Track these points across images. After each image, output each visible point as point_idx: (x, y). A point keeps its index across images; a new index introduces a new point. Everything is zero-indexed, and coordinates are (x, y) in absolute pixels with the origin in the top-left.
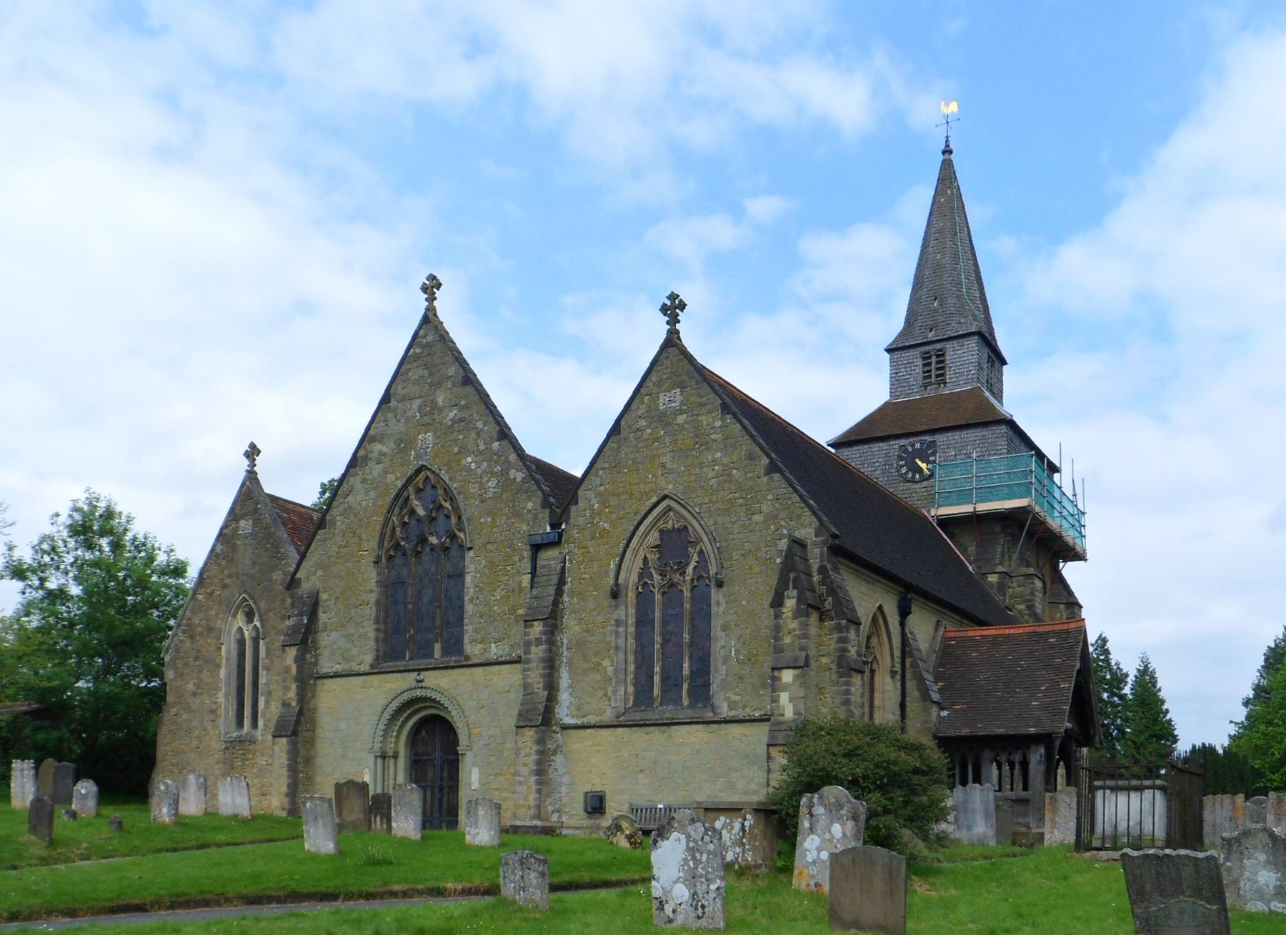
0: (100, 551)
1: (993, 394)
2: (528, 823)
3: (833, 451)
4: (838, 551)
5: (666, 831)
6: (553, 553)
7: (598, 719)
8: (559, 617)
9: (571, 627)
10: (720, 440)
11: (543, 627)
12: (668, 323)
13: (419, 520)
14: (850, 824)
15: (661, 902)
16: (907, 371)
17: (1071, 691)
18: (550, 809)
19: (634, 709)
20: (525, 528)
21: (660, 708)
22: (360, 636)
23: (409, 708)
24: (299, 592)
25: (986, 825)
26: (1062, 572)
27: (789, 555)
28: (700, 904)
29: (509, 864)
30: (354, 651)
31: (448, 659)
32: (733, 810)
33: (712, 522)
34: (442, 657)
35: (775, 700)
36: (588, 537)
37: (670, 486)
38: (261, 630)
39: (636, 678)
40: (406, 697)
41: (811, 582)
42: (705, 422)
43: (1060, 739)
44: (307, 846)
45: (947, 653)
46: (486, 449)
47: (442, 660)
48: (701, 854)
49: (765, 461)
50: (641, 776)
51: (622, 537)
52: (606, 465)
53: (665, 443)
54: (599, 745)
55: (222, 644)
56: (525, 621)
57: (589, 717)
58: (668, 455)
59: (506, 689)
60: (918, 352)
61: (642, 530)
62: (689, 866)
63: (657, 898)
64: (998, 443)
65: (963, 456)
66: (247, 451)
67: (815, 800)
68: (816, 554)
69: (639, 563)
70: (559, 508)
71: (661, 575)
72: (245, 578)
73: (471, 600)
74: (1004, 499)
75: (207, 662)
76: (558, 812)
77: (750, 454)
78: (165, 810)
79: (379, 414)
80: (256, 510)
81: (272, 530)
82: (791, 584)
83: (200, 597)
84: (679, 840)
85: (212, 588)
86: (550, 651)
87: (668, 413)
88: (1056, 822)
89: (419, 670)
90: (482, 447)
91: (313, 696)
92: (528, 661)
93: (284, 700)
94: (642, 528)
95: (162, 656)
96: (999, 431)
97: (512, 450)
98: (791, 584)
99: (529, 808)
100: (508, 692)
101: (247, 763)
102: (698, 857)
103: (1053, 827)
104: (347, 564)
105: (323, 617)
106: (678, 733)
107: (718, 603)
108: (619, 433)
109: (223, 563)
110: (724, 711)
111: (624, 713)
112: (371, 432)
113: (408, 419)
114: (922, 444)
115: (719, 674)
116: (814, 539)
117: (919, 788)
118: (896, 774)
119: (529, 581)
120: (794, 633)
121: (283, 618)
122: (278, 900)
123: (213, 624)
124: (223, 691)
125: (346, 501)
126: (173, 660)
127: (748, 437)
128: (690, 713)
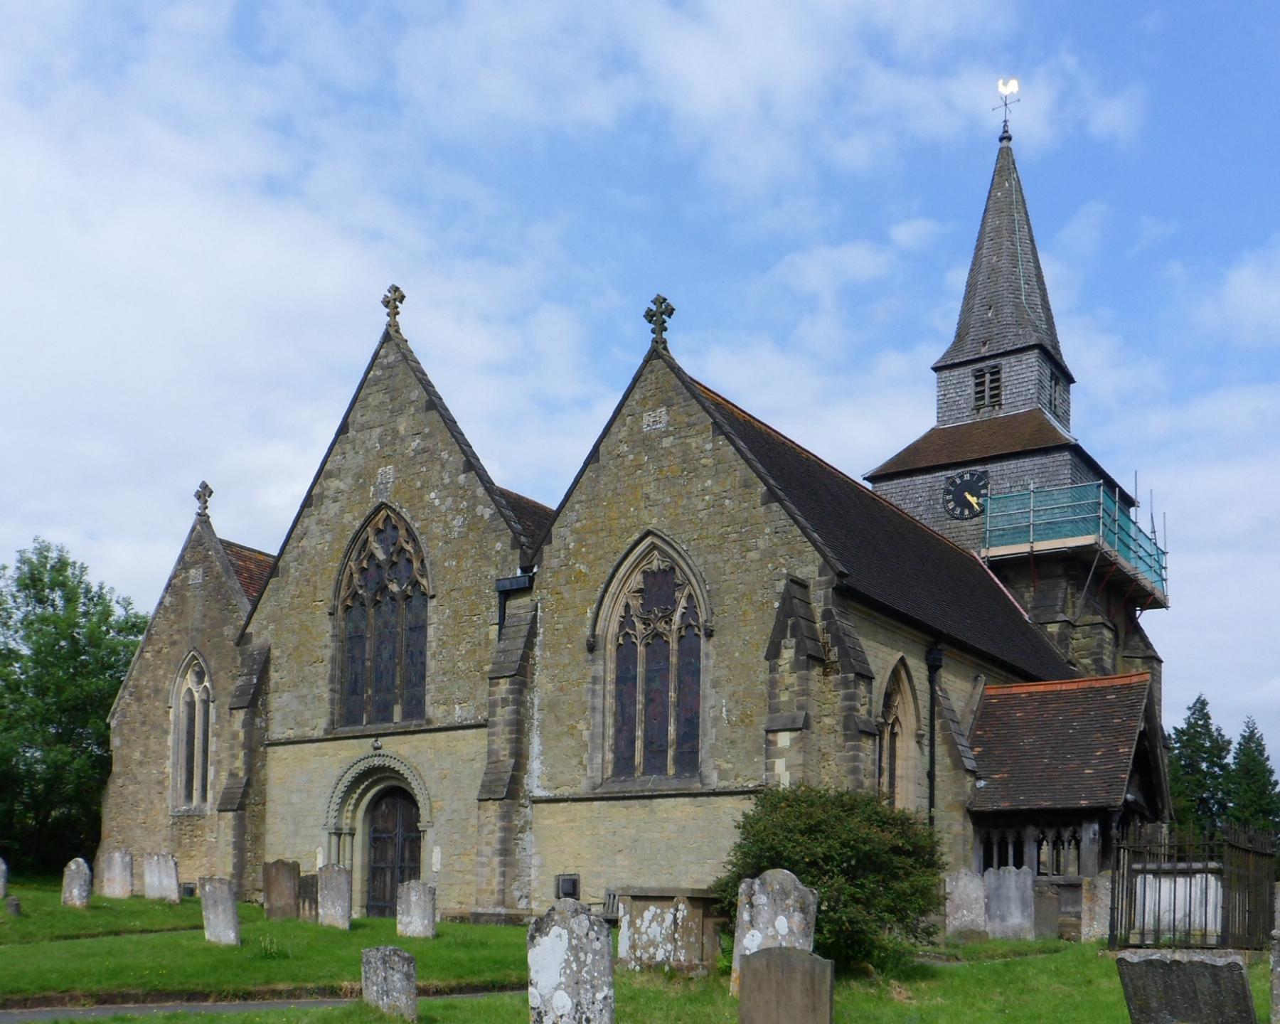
0: (53, 606)
1: (1057, 416)
2: (490, 910)
3: (869, 485)
4: (846, 593)
5: (545, 925)
6: (524, 601)
7: (572, 791)
8: (529, 675)
9: (543, 685)
10: (712, 465)
11: (510, 685)
12: (653, 331)
13: (379, 566)
14: (797, 917)
15: (539, 1014)
16: (956, 392)
17: (1132, 757)
18: (517, 894)
19: (613, 779)
20: (493, 572)
21: (642, 778)
22: (314, 697)
23: (371, 776)
24: (250, 648)
25: (1023, 916)
26: (1139, 620)
27: (786, 598)
28: (584, 1017)
29: (370, 962)
30: (308, 715)
31: (410, 722)
32: (663, 898)
33: (701, 561)
34: (402, 720)
35: (769, 768)
36: (563, 581)
37: (654, 521)
38: (211, 692)
39: (616, 743)
40: (362, 766)
41: (813, 630)
42: (694, 445)
43: (1120, 814)
44: (207, 936)
45: (986, 713)
46: (452, 482)
47: (403, 724)
48: (586, 954)
49: (762, 488)
50: (619, 857)
51: (601, 580)
52: (584, 498)
53: (650, 471)
54: (572, 821)
55: (170, 707)
56: (491, 679)
57: (562, 788)
58: (653, 484)
59: (472, 757)
60: (970, 370)
61: (622, 574)
62: (571, 969)
63: (534, 1009)
64: (1061, 472)
65: (1019, 488)
66: (198, 491)
67: (756, 887)
68: (819, 599)
69: (620, 610)
70: (531, 549)
71: (644, 624)
72: (194, 633)
73: (434, 656)
74: (1067, 536)
75: (154, 727)
76: (527, 897)
77: (745, 481)
78: (76, 892)
79: (337, 446)
80: (207, 557)
81: (223, 579)
82: (789, 631)
83: (148, 655)
84: (560, 936)
85: (160, 646)
86: (517, 712)
87: (653, 435)
88: (1095, 913)
89: (377, 736)
90: (447, 481)
91: (264, 766)
92: (494, 725)
93: (231, 770)
94: (622, 570)
95: (108, 721)
96: (1061, 458)
97: (479, 483)
98: (789, 631)
99: (492, 893)
100: (473, 760)
101: (195, 840)
102: (583, 958)
103: (1092, 919)
104: (301, 616)
105: (274, 676)
106: (662, 808)
107: (707, 655)
108: (598, 461)
109: (172, 617)
110: (714, 782)
111: (602, 784)
112: (328, 467)
113: (367, 450)
114: (972, 475)
115: (708, 739)
116: (818, 578)
117: (901, 872)
118: (868, 855)
119: (497, 632)
120: (791, 690)
121: (234, 678)
122: (136, 999)
123: (160, 686)
124: (171, 760)
125: (300, 545)
126: (119, 725)
127: (742, 461)
128: (675, 785)
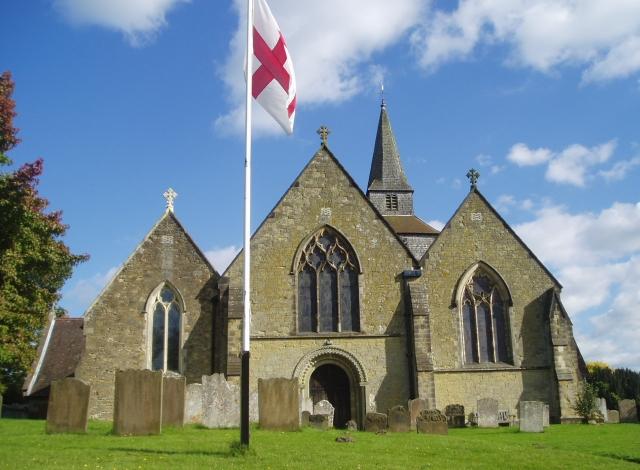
89: (328, 338)
